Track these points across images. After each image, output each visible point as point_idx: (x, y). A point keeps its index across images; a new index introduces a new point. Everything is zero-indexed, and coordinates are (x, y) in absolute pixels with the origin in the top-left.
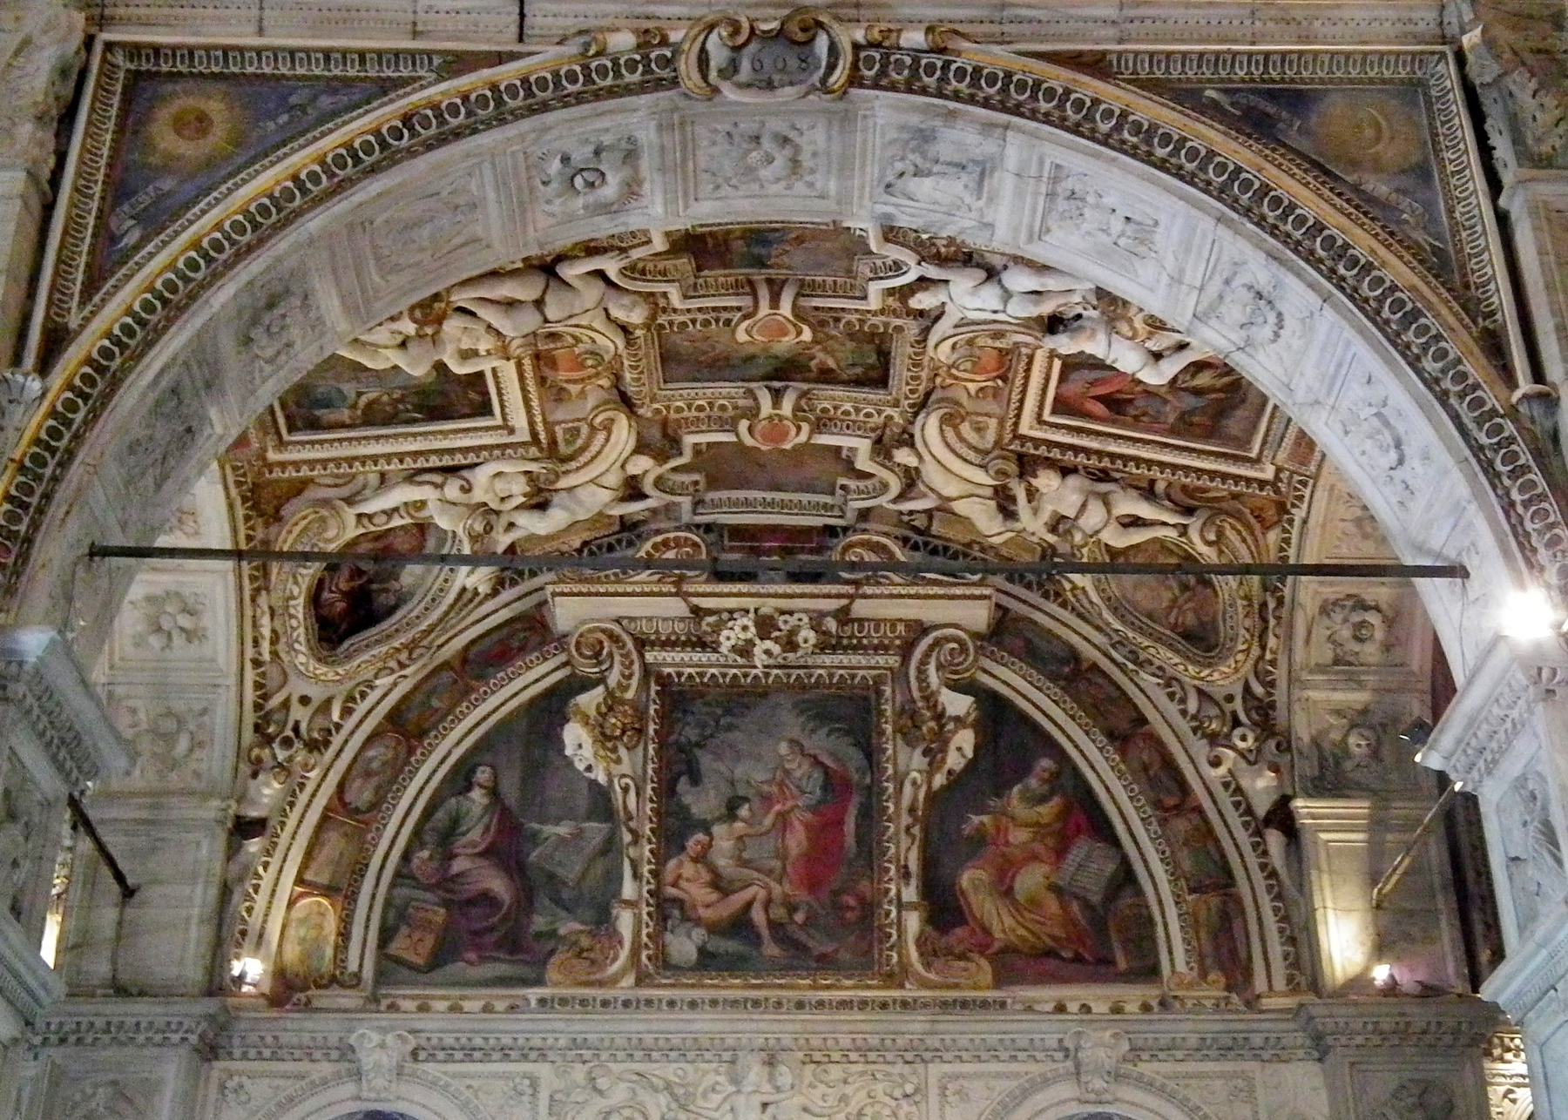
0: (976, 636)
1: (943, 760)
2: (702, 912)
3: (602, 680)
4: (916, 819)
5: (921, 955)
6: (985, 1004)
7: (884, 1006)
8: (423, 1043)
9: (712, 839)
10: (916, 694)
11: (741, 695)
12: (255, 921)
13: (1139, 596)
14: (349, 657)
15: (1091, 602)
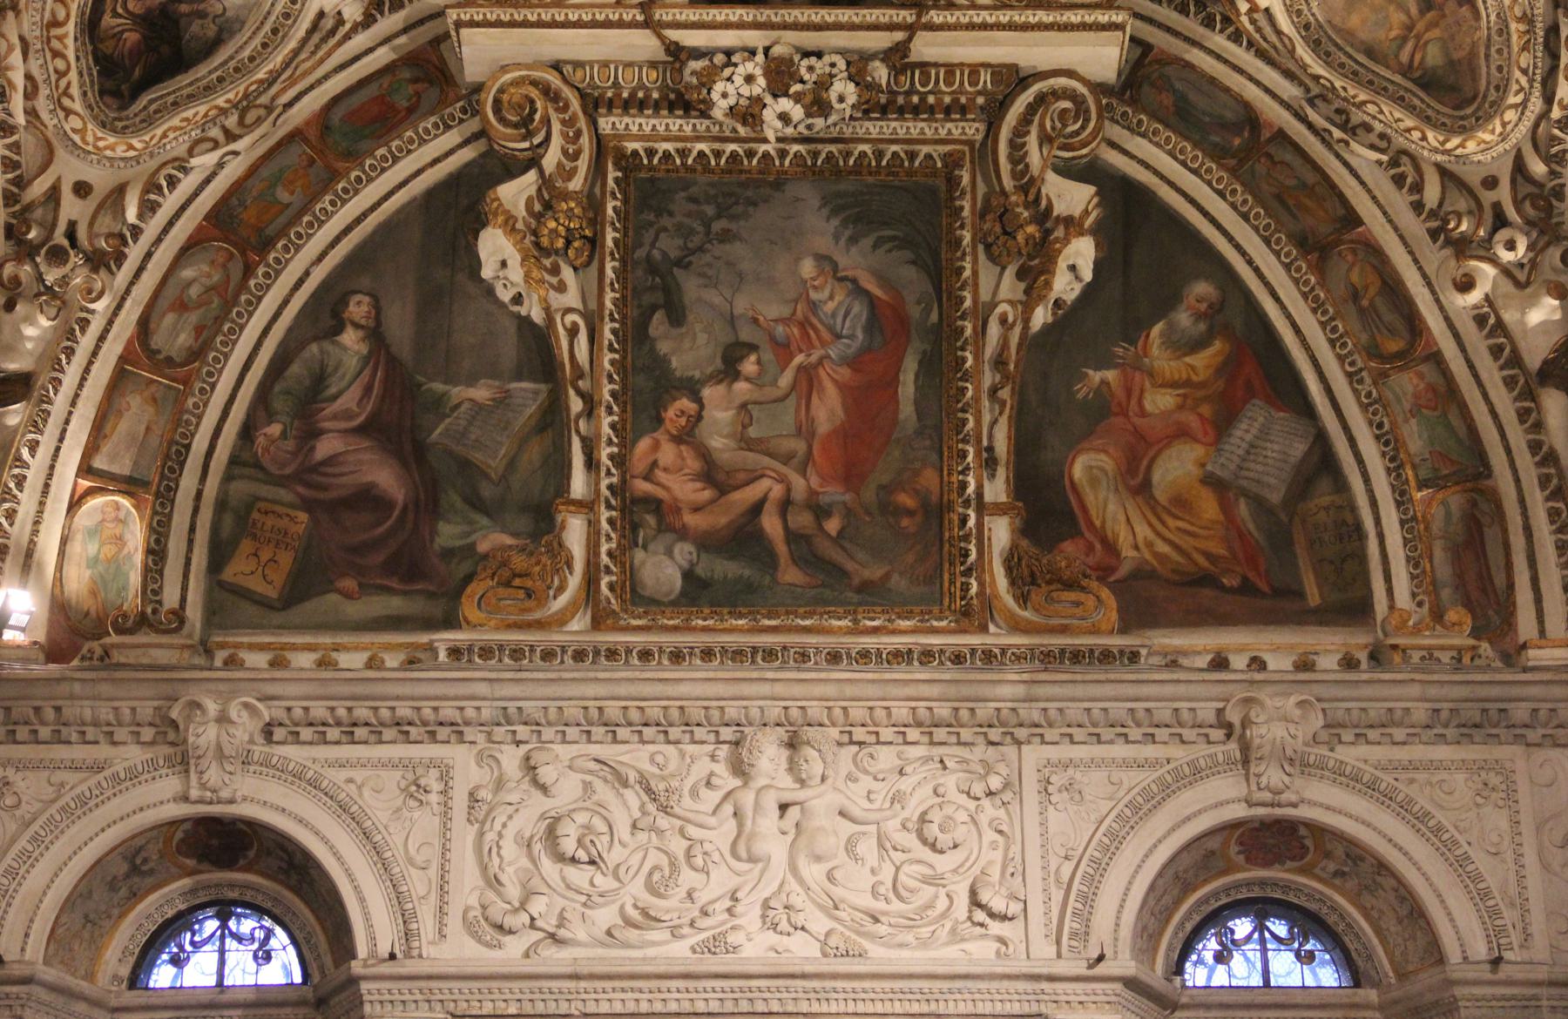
0: (1099, 88)
1: (1048, 285)
2: (690, 519)
3: (534, 162)
4: (1006, 377)
5: (1013, 583)
6: (1106, 656)
7: (958, 659)
8: (280, 714)
9: (702, 406)
10: (1008, 183)
11: (744, 185)
12: (19, 531)
13: (1354, 21)
14: (149, 122)
15: (1279, 33)
